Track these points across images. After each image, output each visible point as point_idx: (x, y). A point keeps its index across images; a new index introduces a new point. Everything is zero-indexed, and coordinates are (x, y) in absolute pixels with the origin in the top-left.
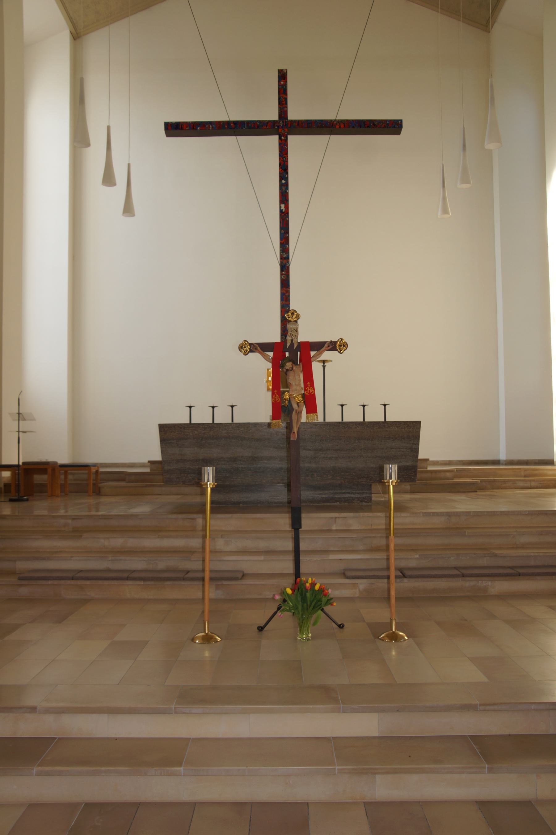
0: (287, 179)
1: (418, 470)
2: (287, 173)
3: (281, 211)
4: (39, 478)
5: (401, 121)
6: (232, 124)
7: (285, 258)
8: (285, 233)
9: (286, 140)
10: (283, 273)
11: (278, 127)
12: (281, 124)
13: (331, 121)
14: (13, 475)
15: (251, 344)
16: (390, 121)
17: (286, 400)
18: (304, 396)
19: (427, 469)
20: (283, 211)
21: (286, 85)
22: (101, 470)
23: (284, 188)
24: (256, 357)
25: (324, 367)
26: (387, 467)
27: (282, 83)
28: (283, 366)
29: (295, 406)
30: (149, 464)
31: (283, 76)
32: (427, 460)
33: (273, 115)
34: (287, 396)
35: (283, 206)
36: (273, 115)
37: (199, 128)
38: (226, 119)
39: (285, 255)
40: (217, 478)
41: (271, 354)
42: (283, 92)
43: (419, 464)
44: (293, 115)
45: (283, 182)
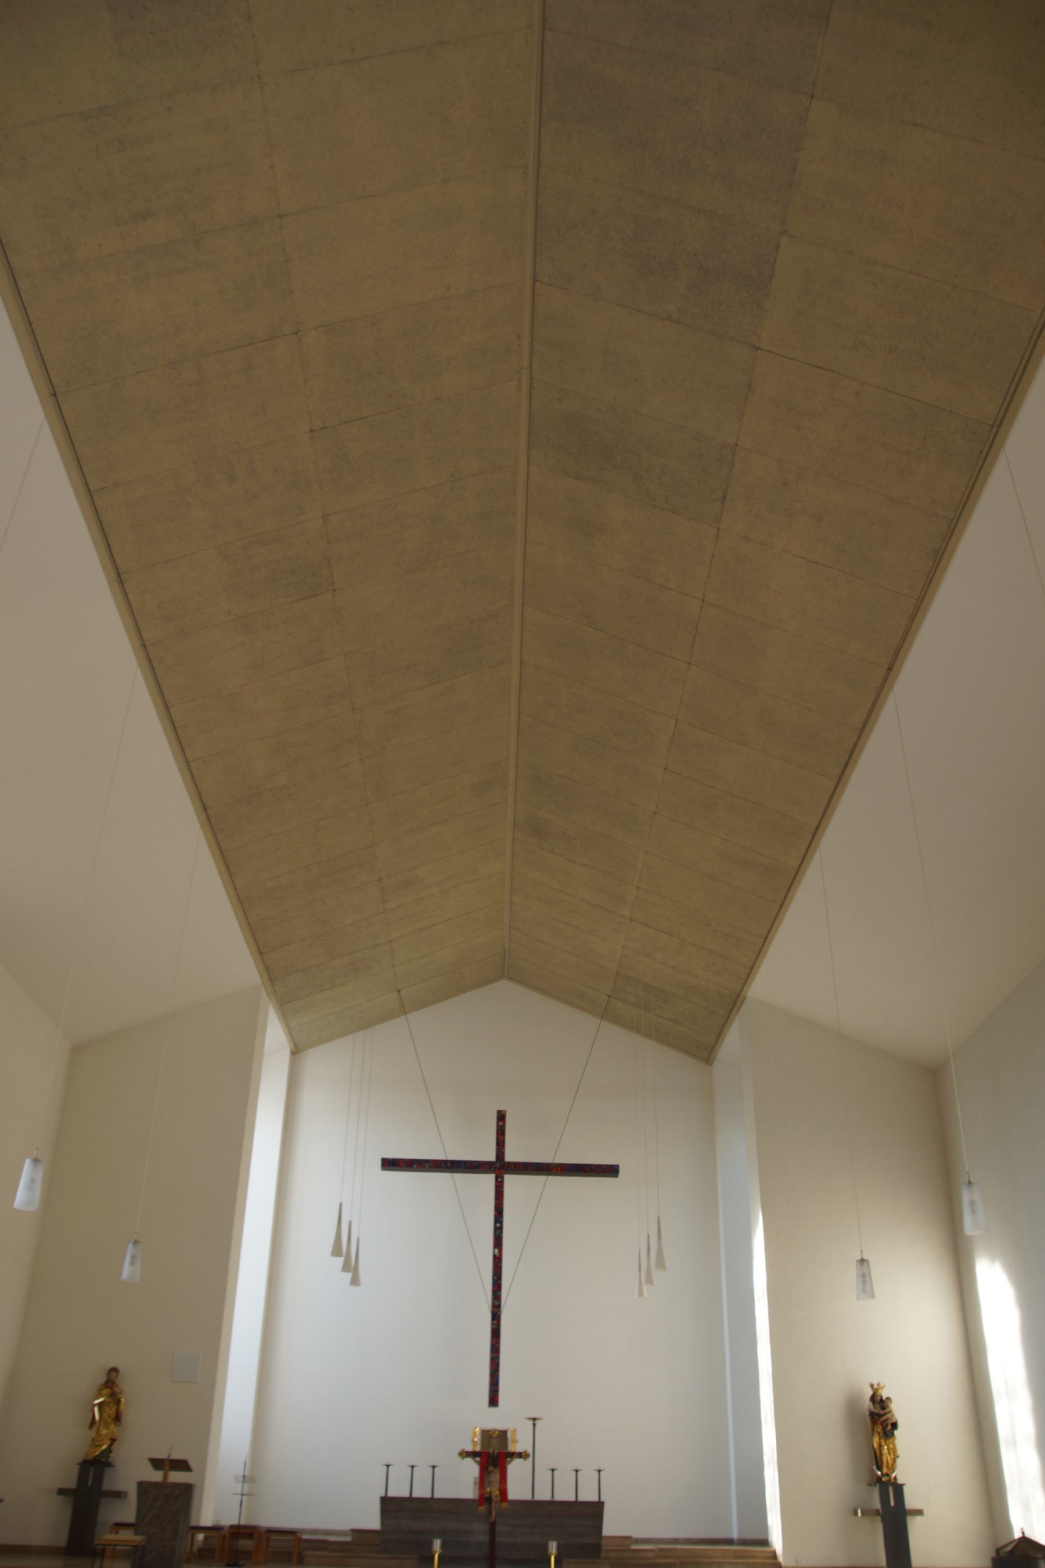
0: (501, 1223)
1: (602, 1548)
2: (502, 1216)
3: (494, 1256)
4: (245, 1544)
5: (618, 1166)
6: (449, 1164)
7: (496, 1307)
8: (497, 1280)
9: (502, 1182)
10: (495, 1322)
11: (495, 1168)
12: (498, 1165)
13: (548, 1164)
14: (206, 1538)
15: (467, 1452)
16: (607, 1166)
17: (487, 1493)
18: (500, 1491)
19: (630, 1546)
20: (497, 1256)
21: (504, 1126)
22: (305, 1537)
23: (498, 1231)
24: (469, 1460)
25: (534, 1425)
26: (550, 1543)
27: (500, 1124)
28: (487, 1469)
29: (493, 1497)
30: (350, 1533)
31: (501, 1117)
32: (629, 1538)
33: (491, 1157)
34: (488, 1490)
35: (497, 1250)
36: (491, 1157)
37: (415, 1166)
38: (444, 1158)
39: (497, 1303)
40: (443, 1545)
41: (478, 1459)
42: (501, 1132)
43: (603, 1542)
44: (510, 1157)
45: (498, 1225)
